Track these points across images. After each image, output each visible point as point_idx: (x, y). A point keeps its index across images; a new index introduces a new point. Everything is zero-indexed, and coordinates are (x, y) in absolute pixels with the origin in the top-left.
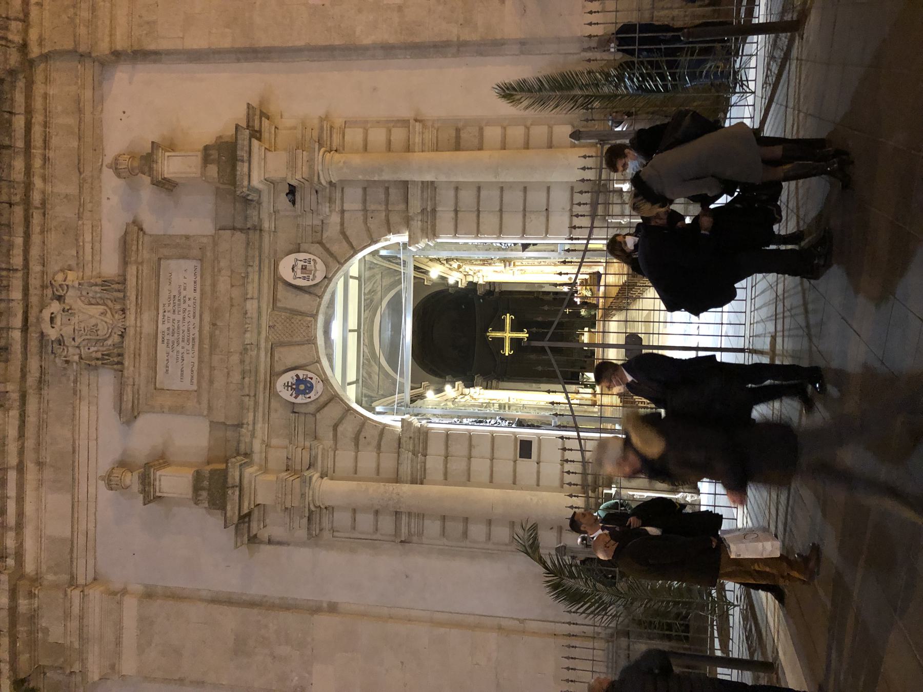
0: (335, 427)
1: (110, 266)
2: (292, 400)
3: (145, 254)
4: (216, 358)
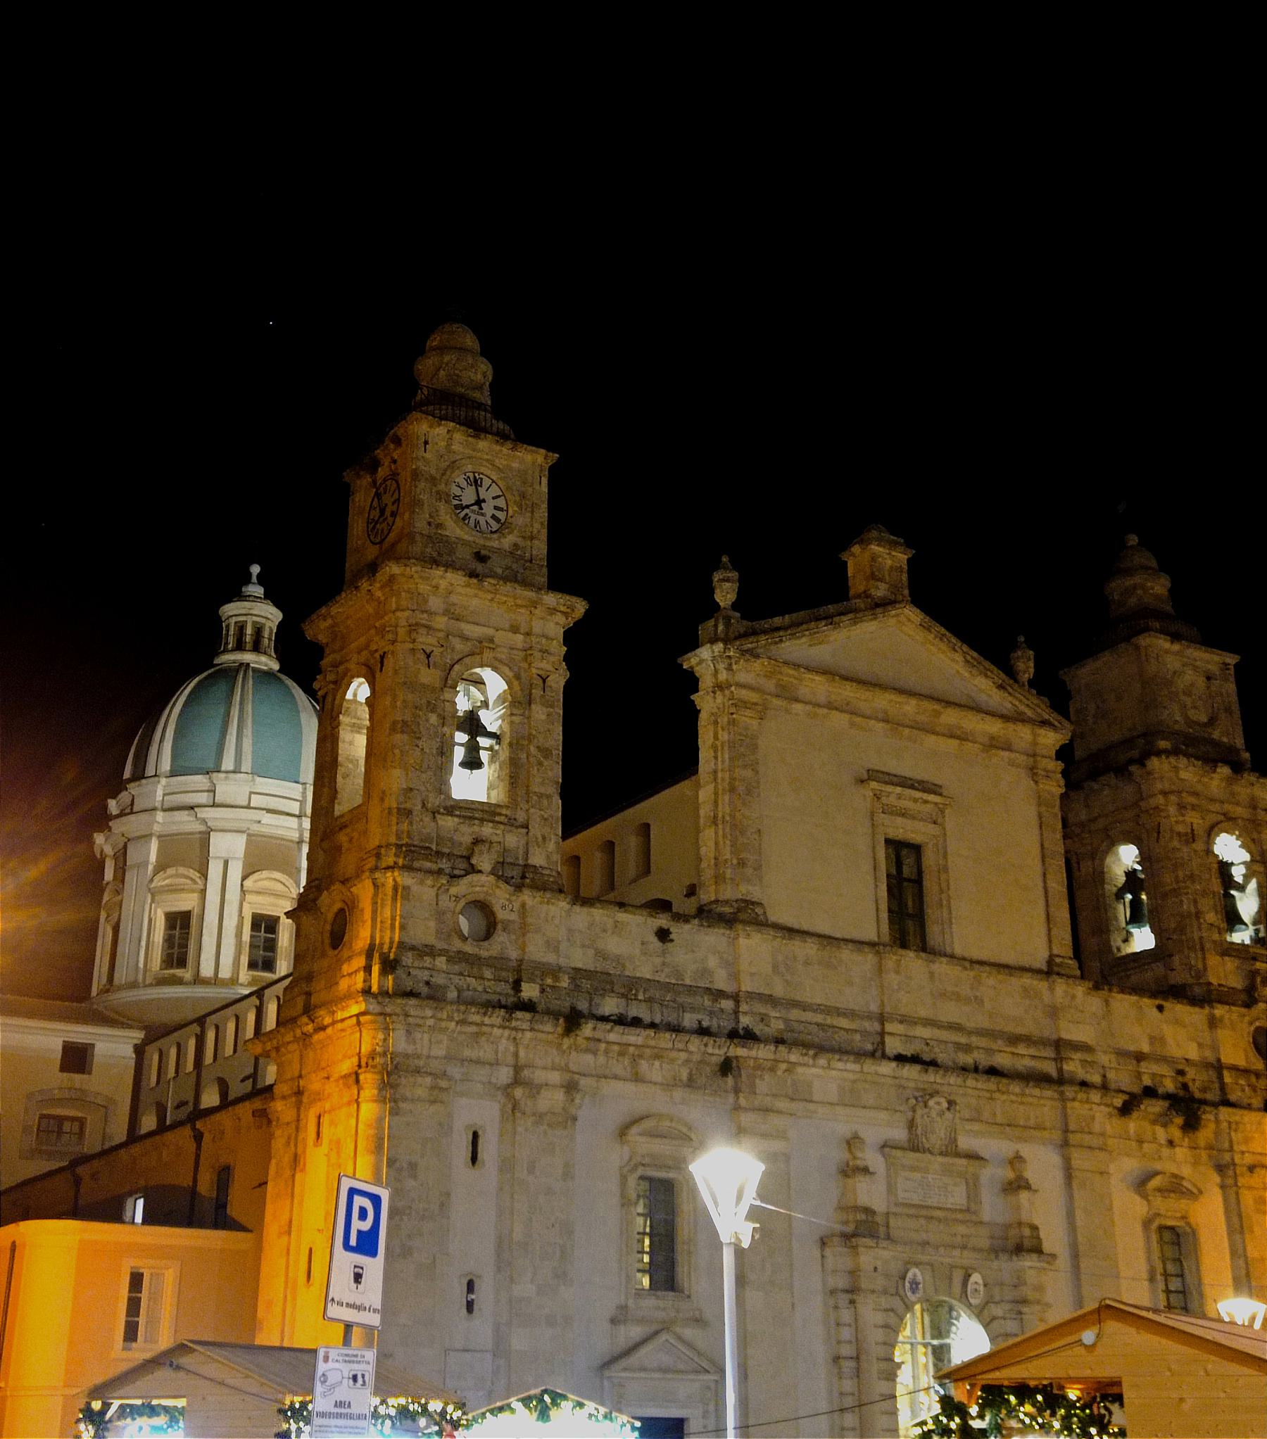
0: (892, 1310)
1: (964, 1143)
2: (907, 1279)
3: (971, 1169)
4: (922, 1221)
